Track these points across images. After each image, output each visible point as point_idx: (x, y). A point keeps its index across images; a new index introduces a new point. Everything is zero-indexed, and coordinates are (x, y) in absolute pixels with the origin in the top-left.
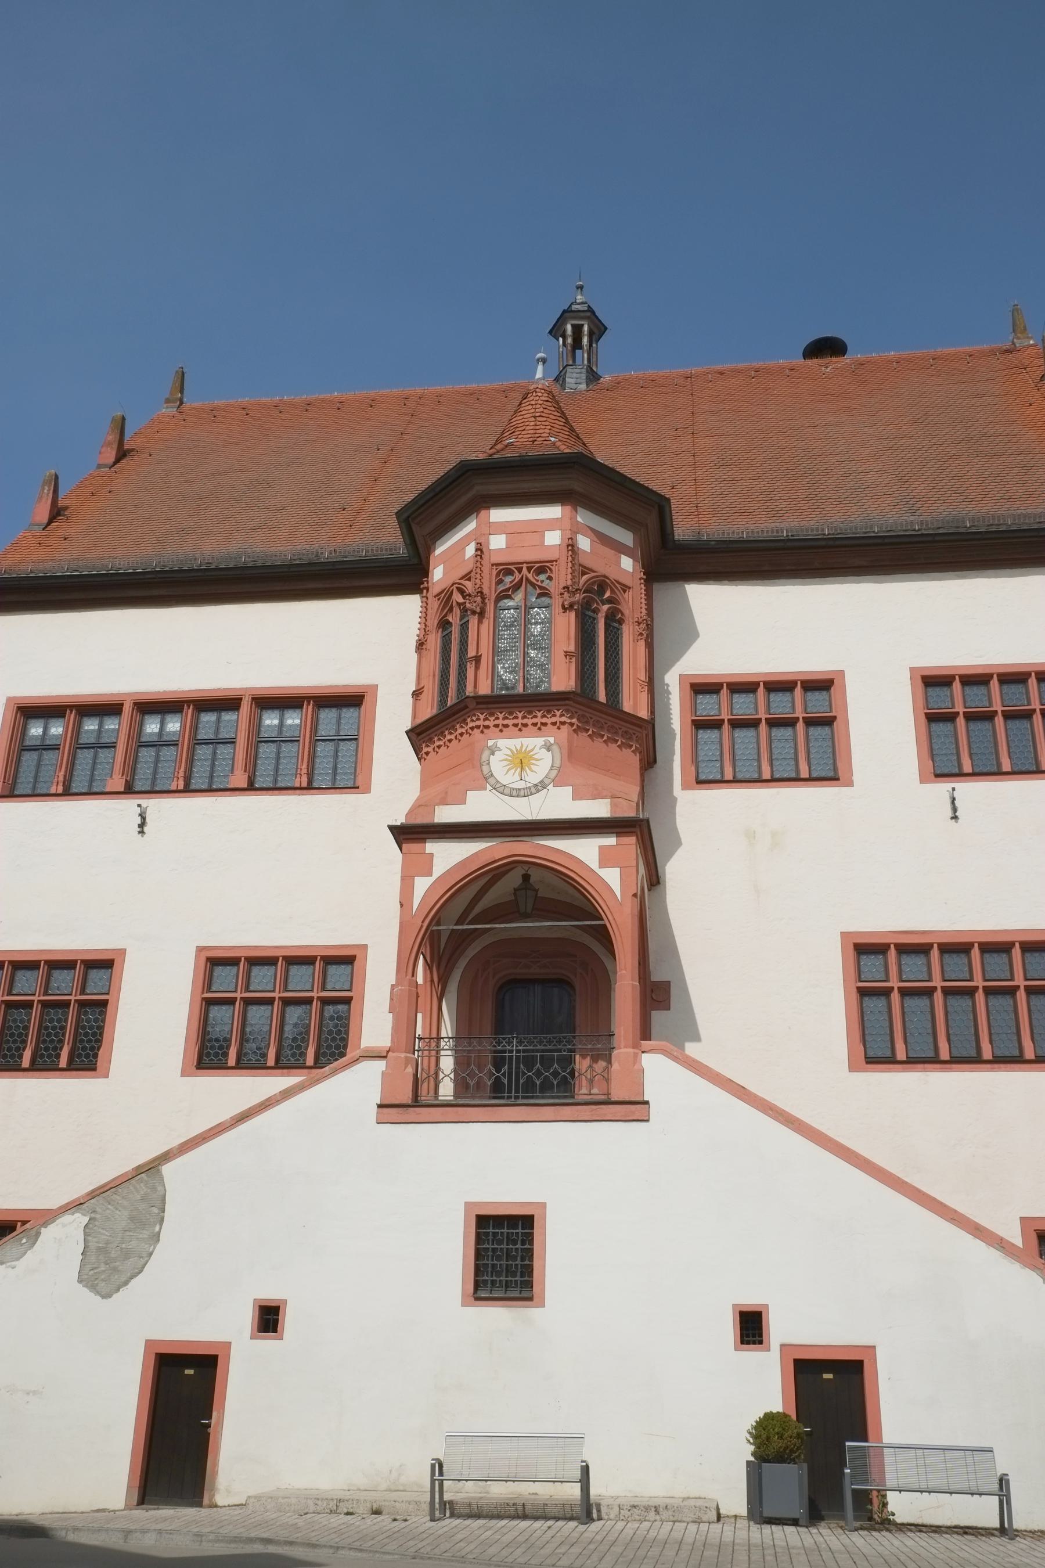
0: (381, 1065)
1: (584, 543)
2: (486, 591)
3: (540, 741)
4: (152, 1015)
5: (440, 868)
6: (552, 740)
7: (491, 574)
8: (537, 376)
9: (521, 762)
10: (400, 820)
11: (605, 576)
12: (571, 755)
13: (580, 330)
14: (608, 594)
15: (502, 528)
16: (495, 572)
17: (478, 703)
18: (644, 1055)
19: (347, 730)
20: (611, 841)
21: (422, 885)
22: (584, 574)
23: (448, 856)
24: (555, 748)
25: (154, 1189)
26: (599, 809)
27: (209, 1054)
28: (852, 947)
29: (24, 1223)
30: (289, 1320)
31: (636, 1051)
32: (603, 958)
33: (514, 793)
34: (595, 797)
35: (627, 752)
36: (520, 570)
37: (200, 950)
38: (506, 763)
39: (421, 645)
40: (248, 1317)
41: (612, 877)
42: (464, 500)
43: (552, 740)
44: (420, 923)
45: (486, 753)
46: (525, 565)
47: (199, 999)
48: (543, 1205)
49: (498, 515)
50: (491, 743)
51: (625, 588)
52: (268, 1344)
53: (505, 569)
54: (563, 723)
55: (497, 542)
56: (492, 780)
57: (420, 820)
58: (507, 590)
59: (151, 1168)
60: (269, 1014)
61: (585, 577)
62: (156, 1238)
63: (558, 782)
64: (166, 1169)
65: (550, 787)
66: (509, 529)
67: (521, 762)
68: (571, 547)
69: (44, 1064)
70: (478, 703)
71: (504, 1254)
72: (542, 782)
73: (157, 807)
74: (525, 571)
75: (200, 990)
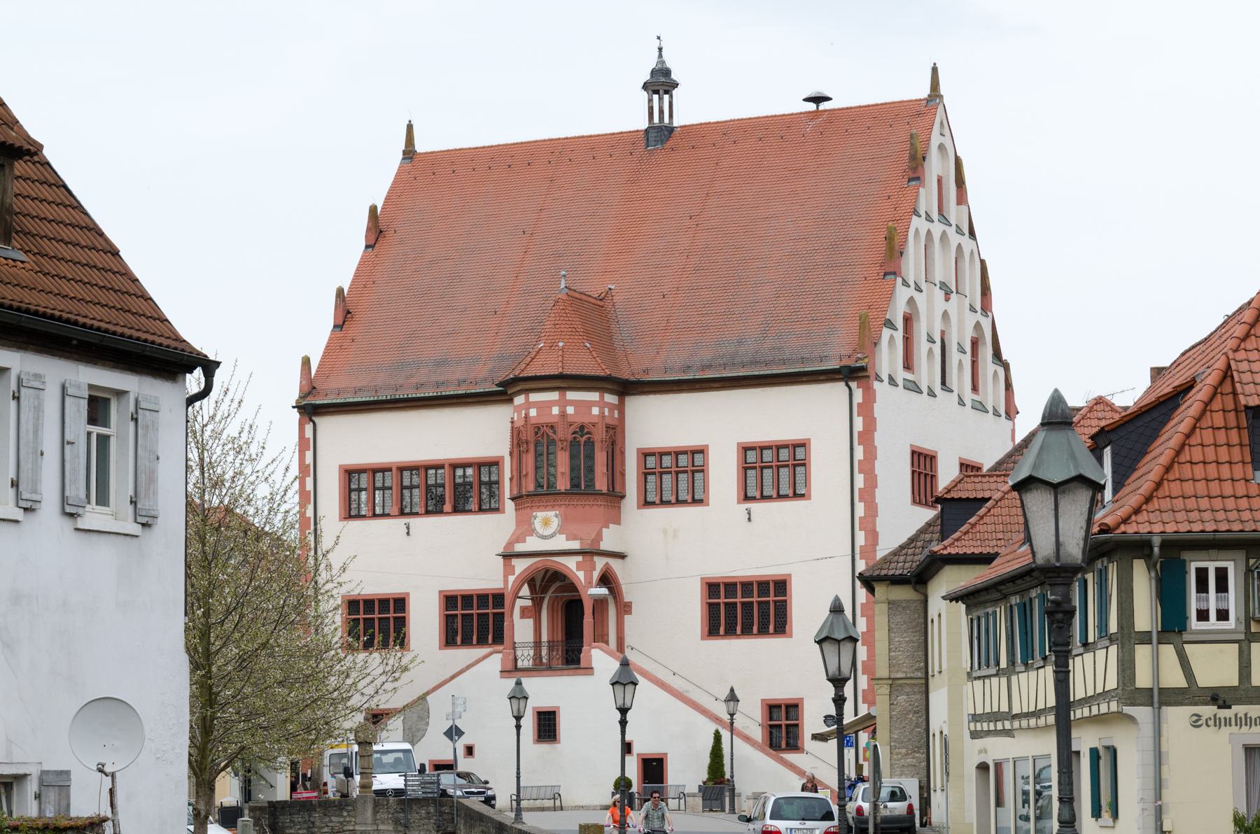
0: (500, 655)
1: (570, 410)
3: (553, 513)
4: (425, 621)
5: (518, 571)
9: (546, 523)
10: (501, 550)
13: (661, 83)
15: (535, 405)
19: (494, 478)
20: (580, 558)
21: (511, 579)
23: (521, 566)
26: (575, 545)
27: (449, 640)
30: (476, 751)
34: (575, 539)
39: (511, 454)
40: (461, 752)
41: (581, 575)
42: (518, 388)
49: (534, 397)
52: (470, 760)
53: (538, 428)
55: (533, 412)
57: (509, 551)
59: (423, 698)
60: (473, 619)
62: (428, 724)
63: (561, 532)
64: (428, 698)
67: (546, 523)
68: (563, 414)
71: (547, 726)
73: (413, 521)
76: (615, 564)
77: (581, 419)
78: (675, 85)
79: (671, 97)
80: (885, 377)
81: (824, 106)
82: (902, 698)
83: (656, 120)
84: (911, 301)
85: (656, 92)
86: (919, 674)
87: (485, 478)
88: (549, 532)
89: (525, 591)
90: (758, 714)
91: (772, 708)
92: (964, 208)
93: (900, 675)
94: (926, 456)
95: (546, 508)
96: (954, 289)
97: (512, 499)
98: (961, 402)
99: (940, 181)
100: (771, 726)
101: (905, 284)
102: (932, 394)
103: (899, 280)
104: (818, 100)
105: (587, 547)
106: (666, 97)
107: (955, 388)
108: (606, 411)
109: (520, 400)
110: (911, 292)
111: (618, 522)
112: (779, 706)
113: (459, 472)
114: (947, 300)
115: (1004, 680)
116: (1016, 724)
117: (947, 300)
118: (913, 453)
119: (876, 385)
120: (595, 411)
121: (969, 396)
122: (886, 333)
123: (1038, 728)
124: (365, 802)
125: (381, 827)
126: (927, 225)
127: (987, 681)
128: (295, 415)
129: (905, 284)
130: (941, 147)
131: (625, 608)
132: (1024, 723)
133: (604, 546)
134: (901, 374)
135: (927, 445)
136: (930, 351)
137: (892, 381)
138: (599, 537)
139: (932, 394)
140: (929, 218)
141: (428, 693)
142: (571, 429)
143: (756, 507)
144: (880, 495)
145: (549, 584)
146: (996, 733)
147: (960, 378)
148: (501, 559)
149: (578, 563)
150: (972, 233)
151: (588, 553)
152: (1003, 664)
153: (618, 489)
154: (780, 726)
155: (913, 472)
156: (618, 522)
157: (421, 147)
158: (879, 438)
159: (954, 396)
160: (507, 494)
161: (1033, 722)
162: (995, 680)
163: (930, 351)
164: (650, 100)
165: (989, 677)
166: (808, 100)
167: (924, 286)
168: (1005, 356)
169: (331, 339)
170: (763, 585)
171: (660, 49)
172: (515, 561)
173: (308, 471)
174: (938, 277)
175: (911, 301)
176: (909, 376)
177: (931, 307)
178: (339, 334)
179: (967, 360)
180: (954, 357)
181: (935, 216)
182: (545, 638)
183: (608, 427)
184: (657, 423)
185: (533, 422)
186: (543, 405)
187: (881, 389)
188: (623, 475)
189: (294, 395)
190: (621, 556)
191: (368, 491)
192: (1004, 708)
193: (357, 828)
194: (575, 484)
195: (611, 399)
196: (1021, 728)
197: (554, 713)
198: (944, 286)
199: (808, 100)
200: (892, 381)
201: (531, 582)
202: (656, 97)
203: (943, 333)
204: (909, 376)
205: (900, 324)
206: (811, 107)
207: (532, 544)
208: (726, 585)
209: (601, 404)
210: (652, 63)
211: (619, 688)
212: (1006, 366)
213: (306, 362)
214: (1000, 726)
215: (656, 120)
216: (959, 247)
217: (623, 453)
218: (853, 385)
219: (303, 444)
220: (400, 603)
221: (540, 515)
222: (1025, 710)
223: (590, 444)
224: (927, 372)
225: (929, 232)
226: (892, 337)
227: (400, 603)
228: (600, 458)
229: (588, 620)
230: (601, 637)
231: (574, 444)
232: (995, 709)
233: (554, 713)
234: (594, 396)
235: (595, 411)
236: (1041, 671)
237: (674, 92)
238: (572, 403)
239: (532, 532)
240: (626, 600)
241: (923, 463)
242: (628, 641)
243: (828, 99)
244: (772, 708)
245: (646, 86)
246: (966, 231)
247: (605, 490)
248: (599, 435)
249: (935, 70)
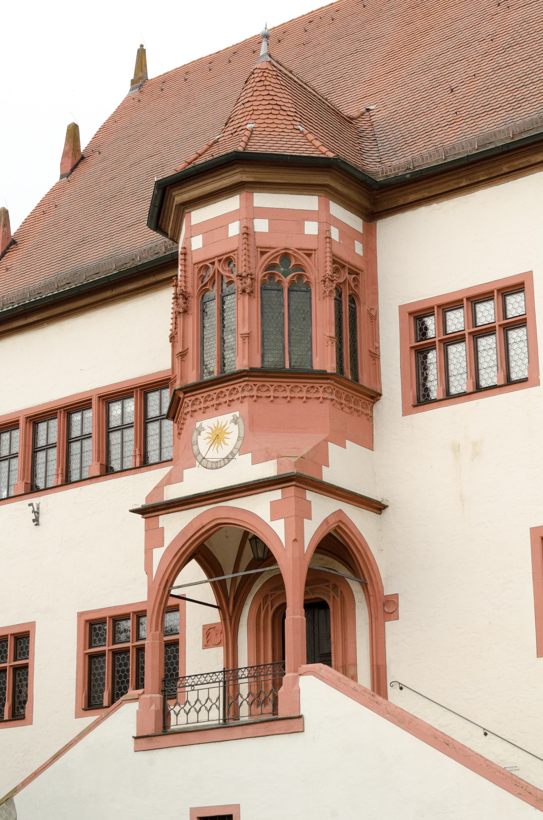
1: (261, 226)
2: (190, 290)
3: (229, 417)
5: (169, 537)
6: (237, 414)
7: (193, 274)
8: (261, 54)
9: (217, 437)
10: (141, 503)
11: (286, 249)
12: (252, 425)
14: (293, 263)
16: (196, 271)
17: (185, 393)
18: (301, 678)
20: (276, 495)
21: (158, 554)
22: (262, 253)
23: (174, 525)
24: (240, 421)
25: (10, 814)
26: (268, 470)
28: (540, 540)
31: (295, 674)
32: (349, 581)
33: (214, 466)
34: (268, 458)
35: (313, 405)
36: (213, 263)
37: (80, 615)
38: (208, 440)
41: (279, 527)
43: (237, 414)
44: (157, 587)
45: (195, 433)
46: (216, 260)
47: (82, 655)
48: (238, 806)
50: (198, 425)
54: (245, 397)
56: (199, 458)
58: (206, 285)
61: (266, 256)
63: (242, 451)
65: (237, 456)
68: (247, 233)
70: (185, 393)
72: (231, 453)
74: (216, 264)
75: (82, 648)
76: (360, 519)
77: (280, 242)
88: (222, 450)
105: (290, 470)
108: (335, 234)
111: (367, 441)
113: (116, 409)
120: (311, 228)
131: (385, 608)
133: (329, 476)
138: (320, 456)
141: (16, 790)
145: (236, 564)
149: (273, 504)
151: (300, 481)
153: (365, 380)
156: (367, 441)
183: (339, 264)
184: (433, 253)
185: (196, 259)
186: (213, 225)
188: (375, 356)
190: (378, 507)
217: (374, 318)
221: (208, 424)
223: (301, 286)
228: (323, 312)
230: (319, 651)
231: (269, 285)
234: (309, 202)
235: (311, 228)
238: (263, 213)
239: (194, 458)
240: (387, 592)
242: (394, 673)
247: (330, 367)
248: (318, 270)
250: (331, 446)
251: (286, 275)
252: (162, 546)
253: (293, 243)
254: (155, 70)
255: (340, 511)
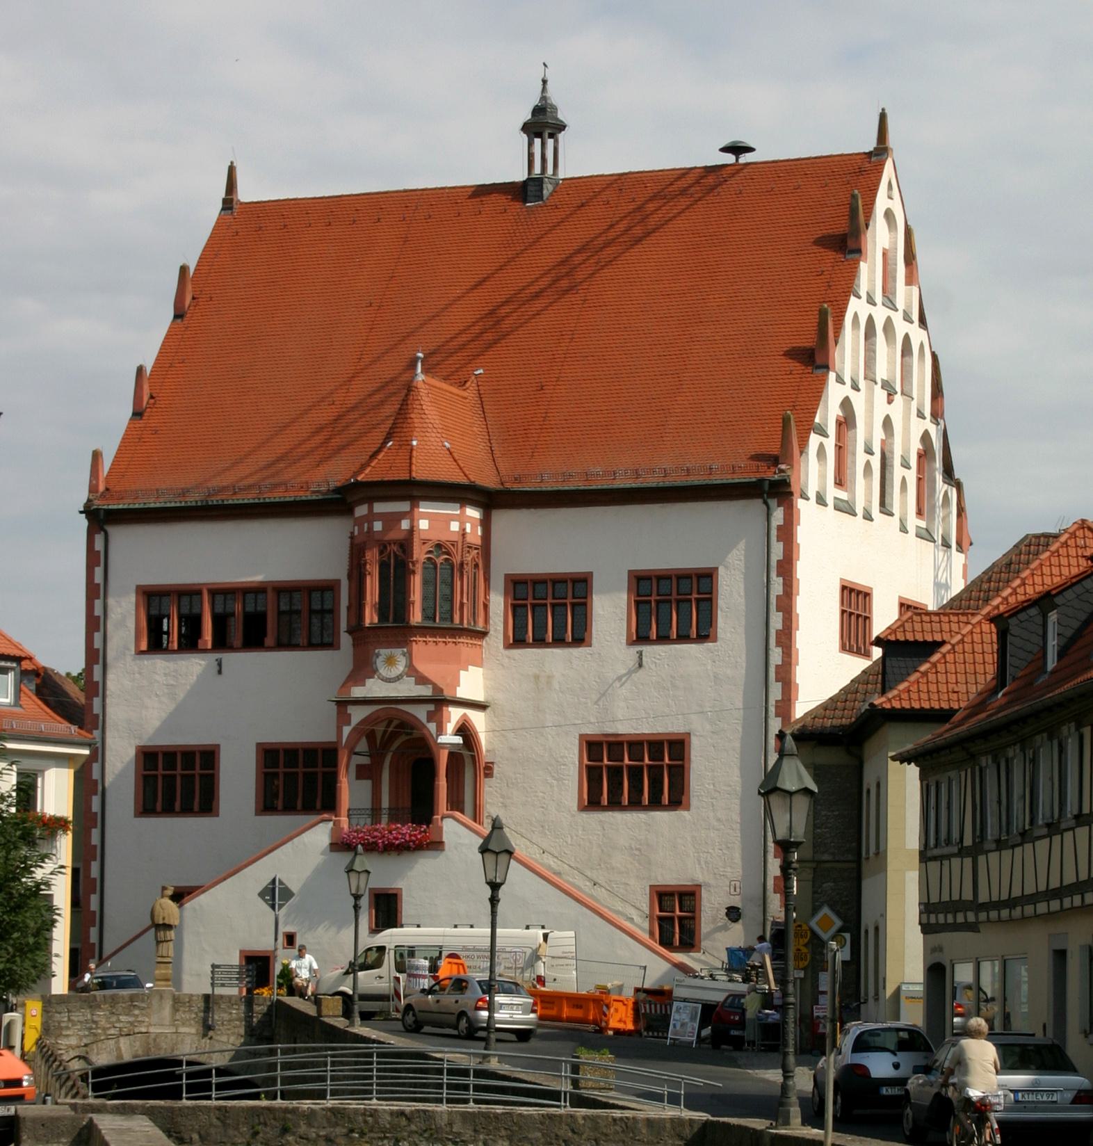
4: (238, 780)
5: (355, 720)
9: (390, 661)
19: (327, 606)
21: (347, 730)
23: (358, 715)
29: (189, 893)
39: (350, 576)
49: (379, 507)
51: (454, 544)
55: (378, 526)
57: (344, 697)
66: (382, 517)
69: (187, 811)
78: (562, 127)
79: (556, 142)
80: (812, 494)
81: (746, 158)
82: (828, 885)
83: (537, 169)
84: (846, 404)
85: (539, 135)
86: (850, 857)
87: (316, 606)
89: (363, 746)
90: (645, 902)
91: (662, 896)
92: (915, 290)
93: (826, 857)
94: (859, 592)
95: (389, 645)
96: (898, 389)
97: (349, 632)
98: (904, 530)
99: (884, 254)
100: (660, 919)
101: (840, 380)
102: (868, 517)
103: (832, 376)
104: (736, 149)
106: (550, 142)
107: (896, 509)
109: (361, 511)
110: (846, 390)
112: (671, 894)
114: (890, 402)
115: (968, 862)
116: (983, 916)
117: (890, 402)
118: (844, 588)
119: (800, 504)
120: (455, 526)
121: (913, 522)
122: (814, 440)
123: (1011, 920)
124: (161, 997)
125: (182, 1030)
126: (869, 309)
127: (946, 863)
128: (83, 522)
129: (840, 380)
130: (889, 215)
132: (993, 914)
133: (462, 693)
134: (832, 493)
135: (860, 579)
136: (868, 465)
137: (821, 500)
139: (868, 517)
140: (871, 301)
142: (427, 547)
143: (647, 650)
144: (802, 639)
146: (956, 927)
147: (905, 501)
148: (334, 707)
149: (429, 713)
150: (923, 321)
152: (968, 841)
154: (672, 919)
155: (843, 612)
157: (246, 194)
158: (802, 570)
159: (895, 520)
160: (343, 625)
161: (1005, 913)
162: (956, 862)
163: (868, 465)
164: (530, 144)
165: (948, 857)
166: (725, 150)
167: (862, 384)
168: (957, 475)
169: (128, 429)
170: (656, 745)
171: (544, 82)
172: (351, 709)
173: (95, 591)
174: (881, 373)
175: (846, 404)
176: (843, 495)
177: (871, 408)
178: (140, 423)
179: (912, 476)
180: (898, 472)
181: (879, 298)
182: (385, 803)
187: (806, 508)
189: (81, 496)
191: (173, 620)
192: (968, 895)
193: (152, 1030)
194: (429, 615)
195: (473, 513)
196: (988, 920)
197: (395, 895)
198: (887, 385)
199: (725, 150)
200: (821, 500)
201: (371, 736)
202: (538, 141)
203: (883, 442)
204: (843, 495)
205: (832, 429)
206: (729, 159)
207: (374, 688)
208: (610, 744)
209: (462, 519)
210: (535, 101)
211: (490, 858)
212: (959, 486)
213: (96, 456)
214: (960, 918)
215: (537, 169)
216: (907, 338)
218: (773, 503)
219: (93, 558)
220: (208, 757)
221: (384, 652)
222: (995, 898)
224: (864, 491)
225: (870, 320)
226: (821, 445)
227: (208, 757)
229: (442, 783)
230: (456, 803)
232: (956, 897)
233: (395, 895)
235: (455, 526)
236: (1018, 850)
237: (561, 136)
239: (372, 672)
241: (855, 601)
243: (750, 150)
244: (662, 896)
245: (526, 128)
246: (915, 317)
249: (883, 117)
250: (462, 673)
251: (438, 557)
252: (349, 723)
253: (443, 537)
254: (246, 194)
255: (465, 715)
